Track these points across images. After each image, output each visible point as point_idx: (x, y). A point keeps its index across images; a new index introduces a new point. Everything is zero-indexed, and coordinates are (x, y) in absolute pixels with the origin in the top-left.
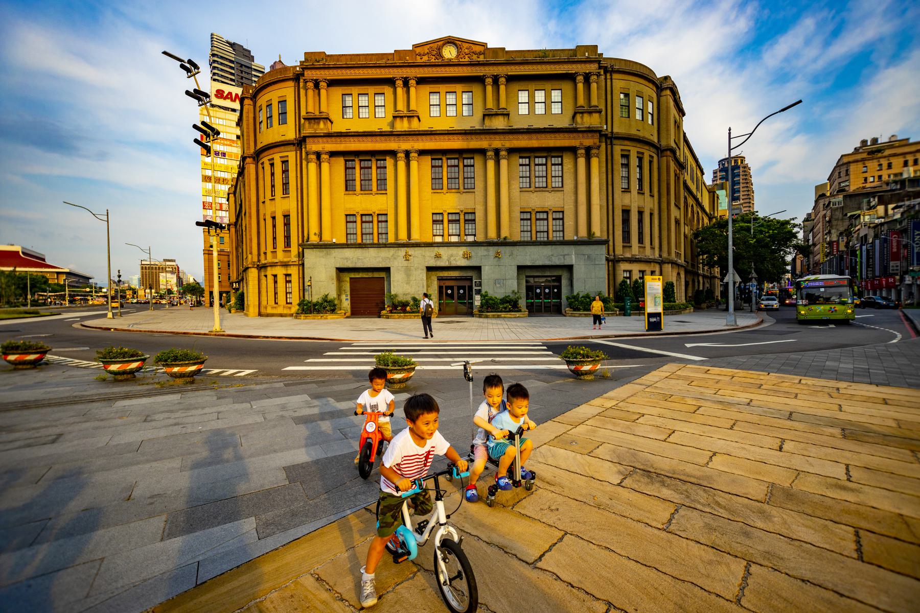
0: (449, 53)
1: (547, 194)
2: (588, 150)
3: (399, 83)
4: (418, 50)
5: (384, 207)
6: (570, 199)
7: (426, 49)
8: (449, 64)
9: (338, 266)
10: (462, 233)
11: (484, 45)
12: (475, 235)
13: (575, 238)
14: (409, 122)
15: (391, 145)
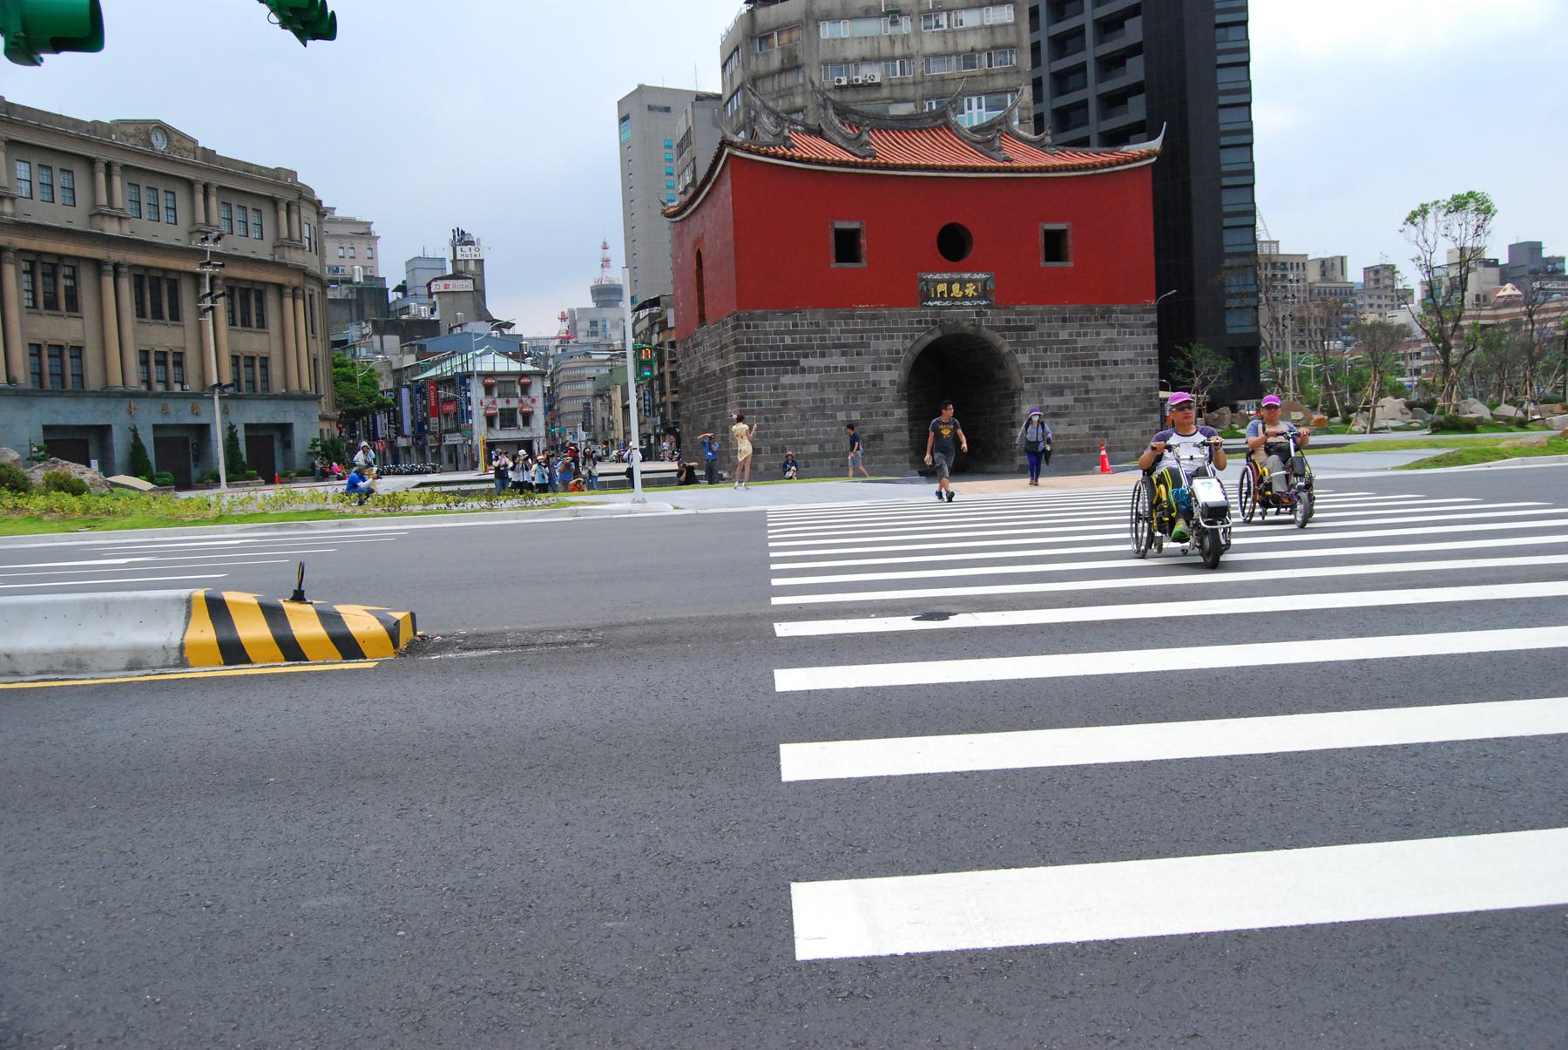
0: (160, 144)
1: (253, 335)
2: (295, 289)
3: (101, 166)
4: (124, 128)
5: (79, 336)
6: (276, 343)
7: (131, 130)
8: (163, 158)
9: (45, 423)
10: (172, 380)
11: (195, 142)
12: (182, 384)
13: (284, 391)
14: (120, 225)
15: (99, 253)
